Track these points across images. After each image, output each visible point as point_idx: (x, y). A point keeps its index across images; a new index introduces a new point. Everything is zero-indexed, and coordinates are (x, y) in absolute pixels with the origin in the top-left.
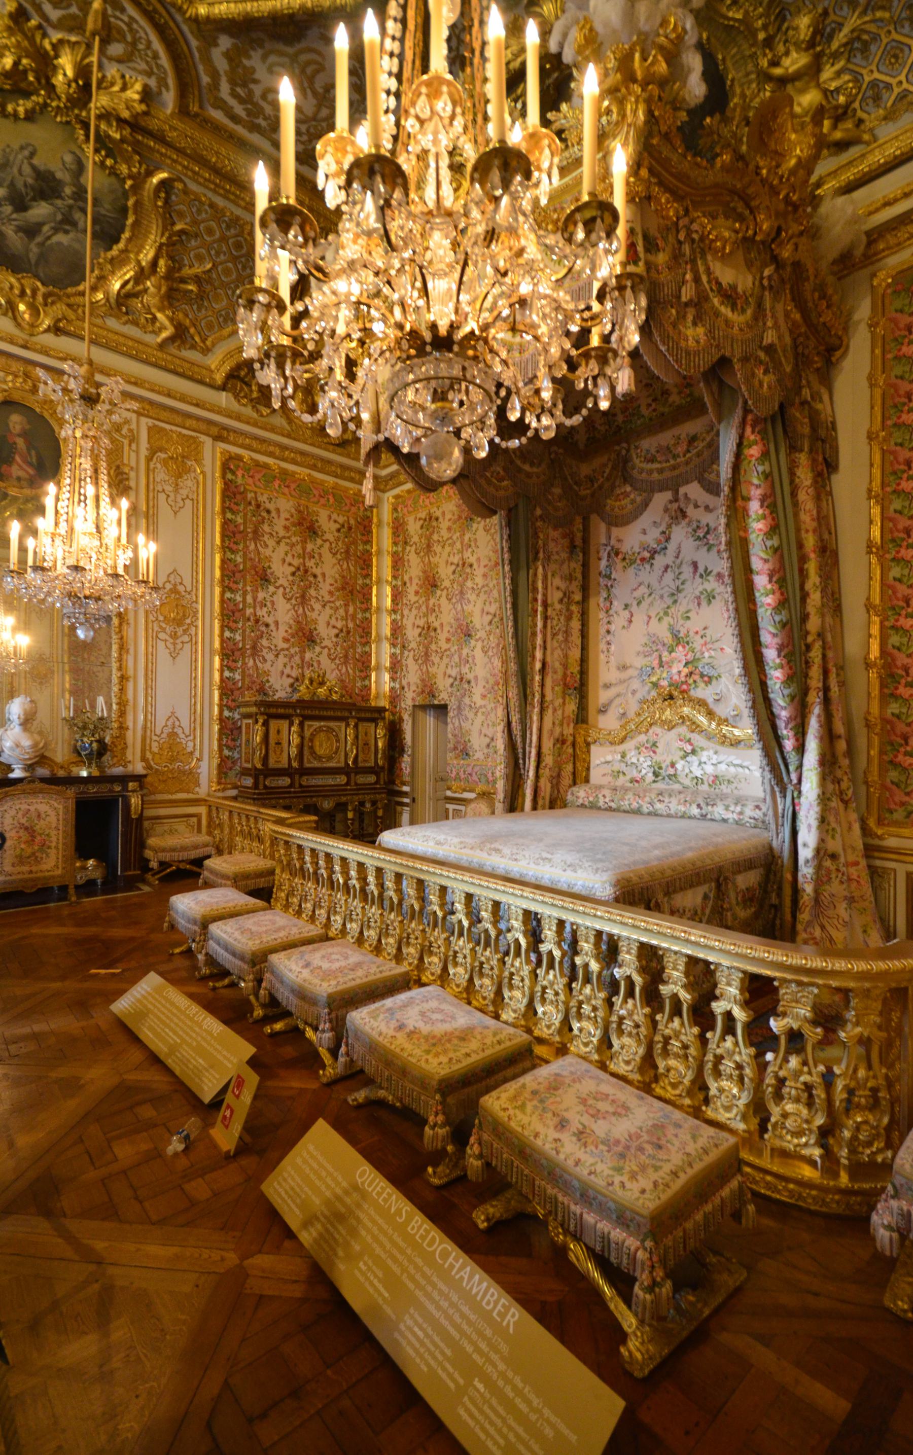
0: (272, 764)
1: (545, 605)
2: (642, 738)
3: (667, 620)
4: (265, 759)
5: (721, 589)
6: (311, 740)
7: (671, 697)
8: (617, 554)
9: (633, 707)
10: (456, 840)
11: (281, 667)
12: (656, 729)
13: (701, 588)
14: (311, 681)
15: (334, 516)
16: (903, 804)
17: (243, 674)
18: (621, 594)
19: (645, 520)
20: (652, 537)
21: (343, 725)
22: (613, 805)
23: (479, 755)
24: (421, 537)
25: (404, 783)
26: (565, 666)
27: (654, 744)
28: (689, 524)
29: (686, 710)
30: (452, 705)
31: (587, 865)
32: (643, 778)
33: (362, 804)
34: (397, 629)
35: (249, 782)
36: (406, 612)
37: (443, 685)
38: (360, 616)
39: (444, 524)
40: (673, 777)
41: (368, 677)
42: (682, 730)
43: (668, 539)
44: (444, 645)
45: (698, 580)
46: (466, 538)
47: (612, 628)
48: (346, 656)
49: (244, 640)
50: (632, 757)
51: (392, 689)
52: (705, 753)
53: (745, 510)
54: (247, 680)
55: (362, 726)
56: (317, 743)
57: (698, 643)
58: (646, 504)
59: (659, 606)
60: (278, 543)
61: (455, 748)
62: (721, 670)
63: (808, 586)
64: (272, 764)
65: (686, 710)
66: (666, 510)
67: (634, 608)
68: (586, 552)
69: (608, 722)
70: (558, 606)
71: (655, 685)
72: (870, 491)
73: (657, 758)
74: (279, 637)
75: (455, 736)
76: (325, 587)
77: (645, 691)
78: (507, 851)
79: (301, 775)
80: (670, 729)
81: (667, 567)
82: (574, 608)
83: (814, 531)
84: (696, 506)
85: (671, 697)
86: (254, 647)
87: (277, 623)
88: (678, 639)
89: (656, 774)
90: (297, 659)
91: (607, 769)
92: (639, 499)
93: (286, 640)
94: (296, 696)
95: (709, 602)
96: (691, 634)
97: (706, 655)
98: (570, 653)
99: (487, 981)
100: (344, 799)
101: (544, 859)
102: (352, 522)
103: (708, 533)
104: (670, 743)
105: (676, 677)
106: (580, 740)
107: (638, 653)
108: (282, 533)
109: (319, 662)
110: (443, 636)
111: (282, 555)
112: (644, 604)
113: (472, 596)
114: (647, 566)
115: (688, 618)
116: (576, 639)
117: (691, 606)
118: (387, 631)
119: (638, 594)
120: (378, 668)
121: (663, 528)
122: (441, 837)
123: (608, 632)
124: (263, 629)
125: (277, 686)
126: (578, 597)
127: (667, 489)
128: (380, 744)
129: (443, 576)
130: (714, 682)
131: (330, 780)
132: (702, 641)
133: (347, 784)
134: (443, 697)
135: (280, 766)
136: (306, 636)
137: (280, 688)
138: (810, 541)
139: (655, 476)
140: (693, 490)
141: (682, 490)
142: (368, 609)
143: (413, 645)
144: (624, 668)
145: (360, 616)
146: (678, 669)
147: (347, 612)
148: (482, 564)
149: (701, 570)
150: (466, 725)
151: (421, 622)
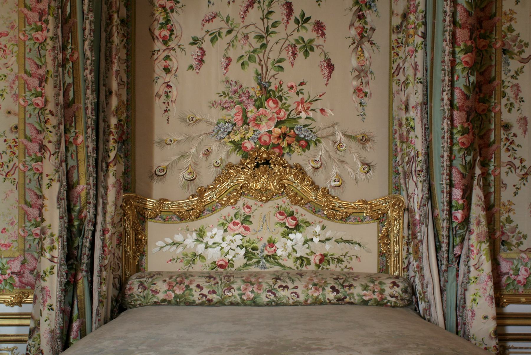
2: (228, 211)
3: (253, 68)
13: (296, 35)
27: (246, 219)
32: (230, 263)
40: (273, 258)
45: (292, 25)
47: (173, 65)
50: (215, 234)
52: (310, 229)
57: (292, 99)
59: (242, 49)
67: (206, 45)
71: (238, 146)
80: (267, 201)
85: (267, 163)
88: (267, 93)
95: (306, 54)
96: (285, 88)
97: (303, 115)
105: (265, 138)
107: (213, 104)
117: (284, 55)
119: (213, 26)
123: (167, 70)
130: (312, 145)
144: (193, 121)
149: (297, 14)
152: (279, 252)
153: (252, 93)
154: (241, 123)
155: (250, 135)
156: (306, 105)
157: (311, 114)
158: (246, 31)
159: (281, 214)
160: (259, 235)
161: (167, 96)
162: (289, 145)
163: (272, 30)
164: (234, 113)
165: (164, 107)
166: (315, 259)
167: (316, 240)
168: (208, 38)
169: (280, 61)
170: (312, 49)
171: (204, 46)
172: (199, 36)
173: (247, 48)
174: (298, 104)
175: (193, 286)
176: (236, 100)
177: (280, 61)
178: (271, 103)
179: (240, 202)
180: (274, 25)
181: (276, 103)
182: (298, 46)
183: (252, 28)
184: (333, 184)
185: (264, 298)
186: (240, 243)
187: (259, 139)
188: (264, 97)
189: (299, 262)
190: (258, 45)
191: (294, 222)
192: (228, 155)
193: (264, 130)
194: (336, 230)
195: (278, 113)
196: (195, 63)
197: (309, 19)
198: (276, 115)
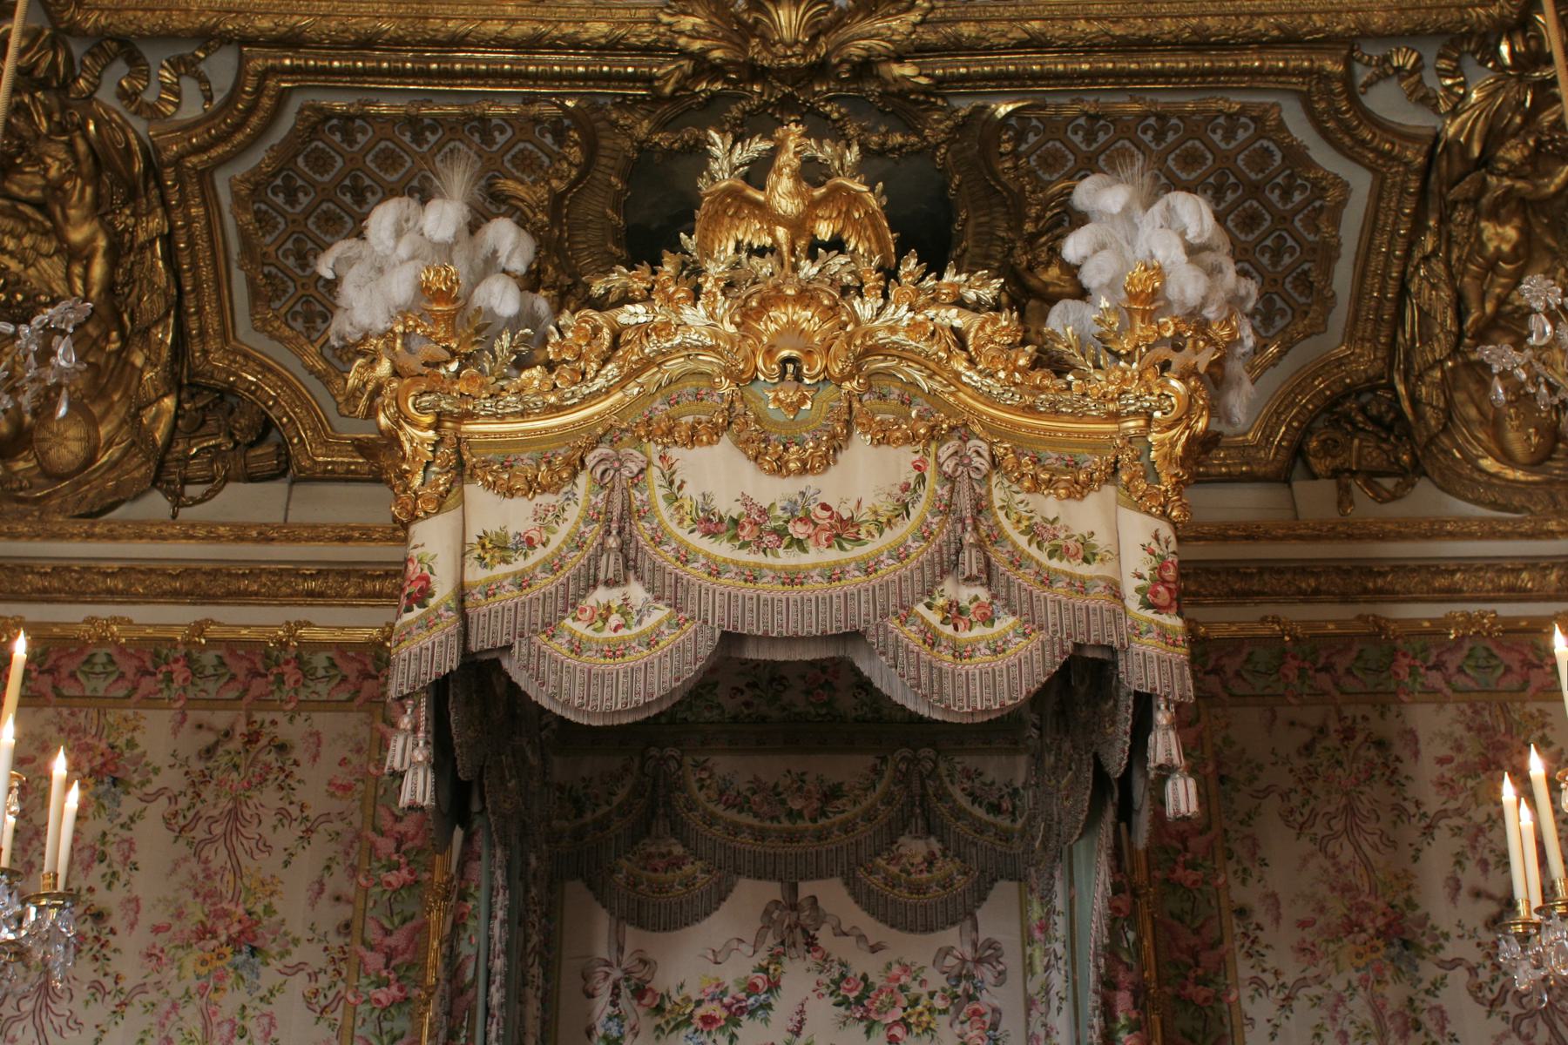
19: (715, 929)
43: (774, 986)
58: (719, 895)
121: (762, 957)
127: (772, 876)
139: (745, 841)
140: (831, 894)
141: (806, 889)
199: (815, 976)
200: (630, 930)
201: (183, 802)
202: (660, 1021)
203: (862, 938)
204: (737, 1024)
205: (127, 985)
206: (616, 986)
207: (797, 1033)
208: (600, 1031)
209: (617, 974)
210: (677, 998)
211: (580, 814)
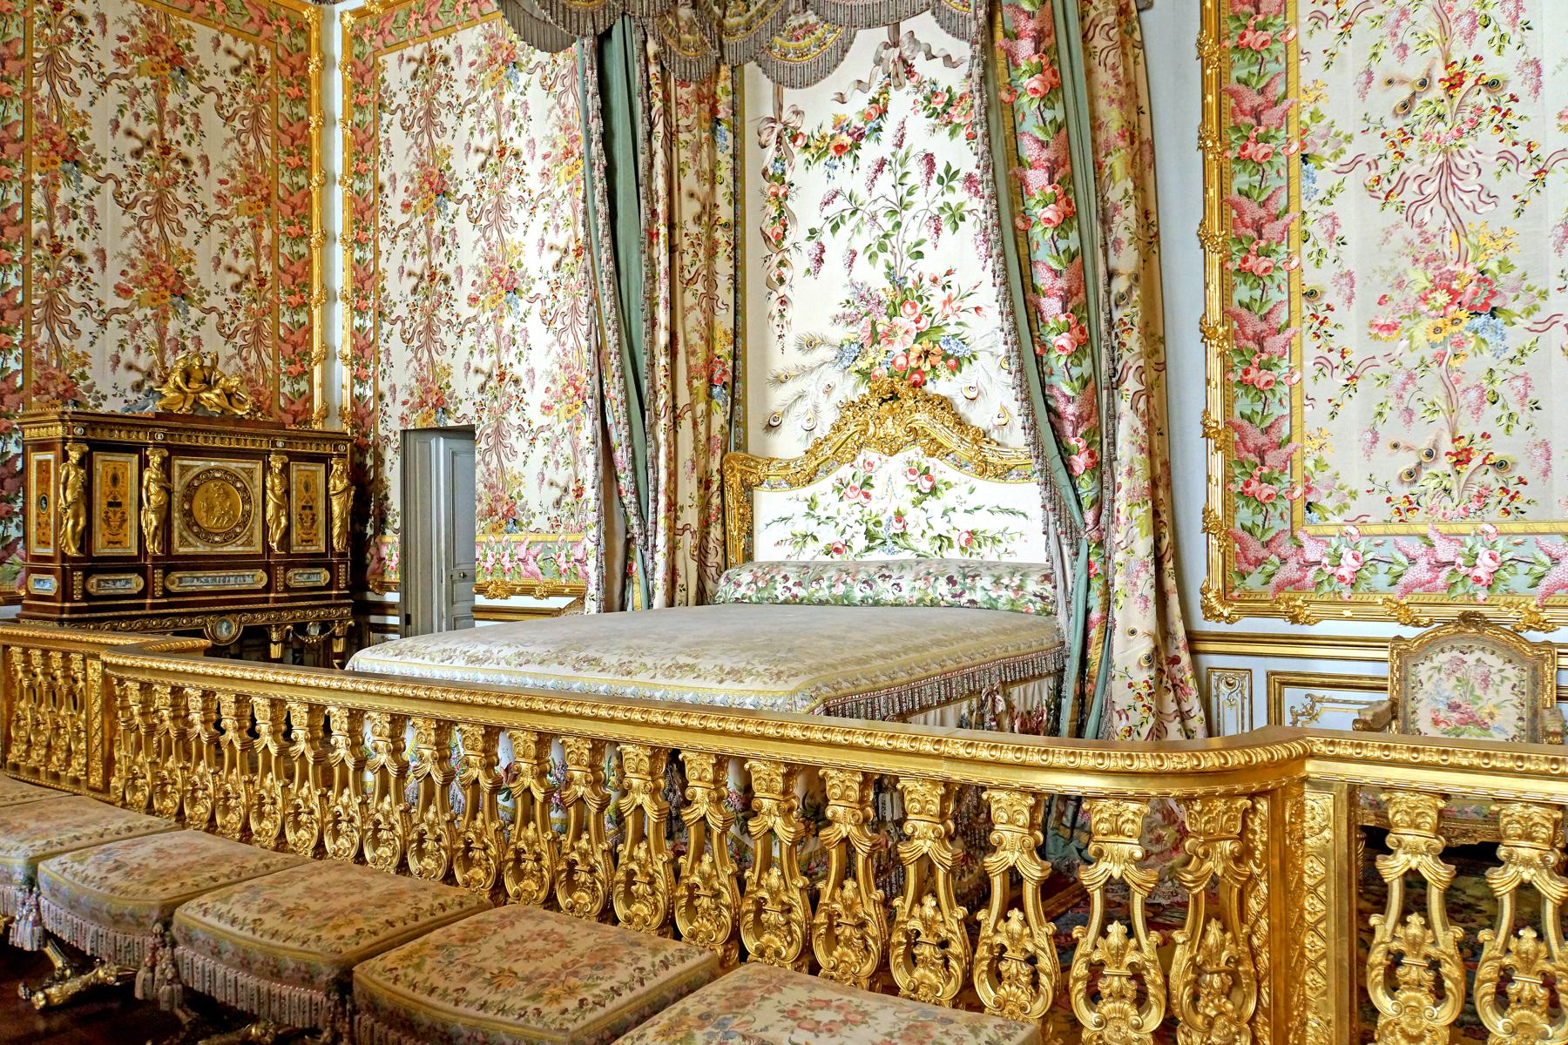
0: (101, 547)
1: (671, 226)
2: (845, 472)
3: (882, 256)
4: (85, 538)
5: (977, 204)
6: (189, 496)
7: (894, 396)
8: (794, 138)
9: (829, 417)
10: (508, 652)
11: (112, 348)
12: (870, 454)
14: (187, 376)
15: (227, 40)
16: (1259, 562)
17: (26, 358)
18: (806, 209)
20: (857, 105)
21: (258, 467)
22: (801, 592)
23: (540, 522)
24: (413, 94)
25: (384, 587)
26: (709, 342)
27: (867, 483)
28: (918, 87)
29: (922, 418)
30: (484, 427)
31: (761, 668)
33: (301, 628)
34: (365, 280)
35: (50, 585)
36: (384, 245)
37: (464, 387)
38: (286, 250)
39: (462, 73)
41: (306, 374)
42: (914, 453)
43: (883, 113)
44: (466, 311)
46: (507, 100)
48: (257, 330)
49: (25, 287)
51: (356, 400)
53: (1012, 58)
54: (35, 373)
55: (298, 471)
56: (199, 504)
57: (937, 298)
59: (868, 236)
60: (103, 86)
61: (492, 512)
62: (976, 345)
63: (1114, 195)
64: (101, 547)
65: (922, 418)
66: (879, 61)
67: (826, 238)
68: (737, 133)
69: (788, 444)
70: (693, 229)
72: (1200, 45)
73: (874, 506)
74: (105, 284)
75: (491, 487)
76: (208, 188)
77: (850, 388)
78: (610, 660)
79: (168, 570)
81: (882, 163)
82: (720, 235)
83: (1121, 103)
84: (930, 56)
85: (894, 396)
86: (50, 303)
87: (101, 254)
88: (904, 295)
89: (870, 536)
90: (149, 331)
91: (783, 531)
92: (831, 38)
93: (123, 292)
94: (154, 407)
96: (926, 282)
97: (952, 320)
98: (717, 320)
99: (584, 897)
100: (260, 619)
101: (680, 667)
102: (265, 55)
103: (949, 104)
104: (891, 476)
105: (901, 361)
106: (734, 480)
108: (111, 67)
109: (198, 342)
110: (462, 292)
111: (112, 113)
112: (844, 230)
113: (521, 216)
114: (848, 160)
115: (920, 255)
116: (724, 293)
118: (341, 279)
120: (327, 355)
121: (873, 92)
122: (480, 649)
123: (781, 281)
124: (72, 265)
125: (104, 387)
126: (725, 213)
128: (336, 509)
129: (461, 175)
130: (966, 364)
131: (234, 580)
132: (944, 296)
133: (267, 589)
134: (464, 412)
135: (118, 551)
136: (169, 285)
137: (112, 392)
138: (1113, 118)
141: (905, 27)
142: (303, 237)
143: (401, 311)
144: (810, 345)
145: (286, 250)
146: (902, 347)
147: (257, 240)
148: (540, 152)
149: (940, 169)
150: (514, 466)
151: (418, 266)
152: (908, 530)
153: (883, 296)
154: (868, 343)
155: (881, 358)
156: (955, 305)
157: (963, 317)
158: (873, 208)
159: (912, 472)
160: (883, 505)
161: (782, 316)
162: (933, 367)
163: (907, 200)
164: (861, 330)
165: (778, 331)
166: (959, 539)
167: (960, 510)
168: (828, 227)
169: (918, 244)
170: (962, 219)
171: (823, 240)
172: (817, 227)
173: (878, 233)
174: (945, 304)
175: (779, 578)
176: (863, 310)
177: (918, 244)
178: (908, 306)
179: (860, 459)
180: (910, 193)
181: (914, 306)
182: (943, 217)
183: (882, 202)
184: (998, 422)
185: (858, 596)
186: (859, 516)
187: (893, 362)
188: (898, 301)
189: (938, 543)
190: (887, 225)
191: (928, 484)
192: (856, 387)
193: (897, 349)
194: (991, 491)
195: (917, 321)
196: (811, 265)
197: (957, 172)
198: (914, 325)
199: (913, 97)
200: (786, 91)
201: (549, 68)
202: (807, 155)
203: (947, 58)
204: (858, 148)
205: (535, 195)
206: (779, 136)
207: (899, 146)
208: (771, 172)
209: (779, 127)
210: (817, 136)
211: (748, 10)
